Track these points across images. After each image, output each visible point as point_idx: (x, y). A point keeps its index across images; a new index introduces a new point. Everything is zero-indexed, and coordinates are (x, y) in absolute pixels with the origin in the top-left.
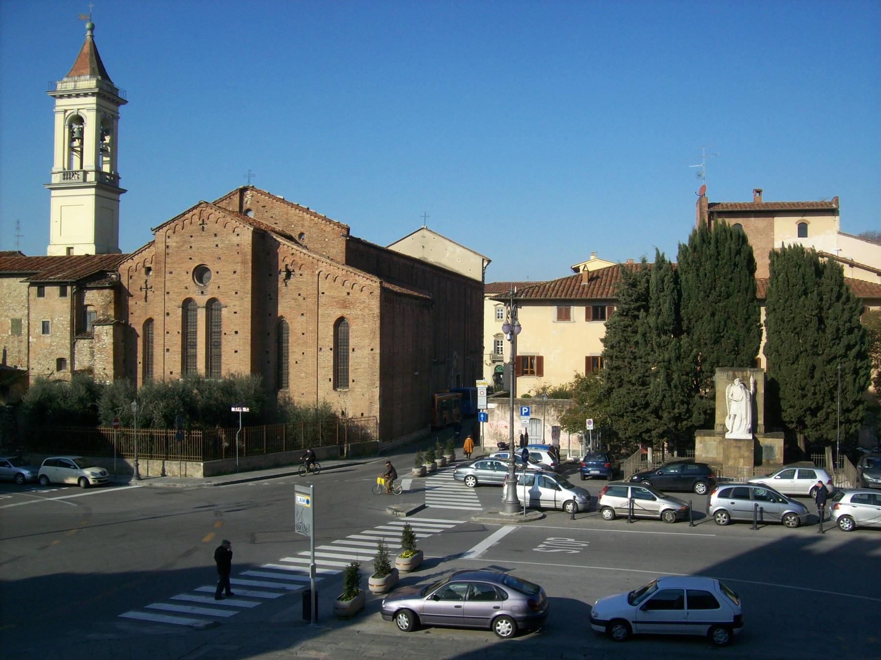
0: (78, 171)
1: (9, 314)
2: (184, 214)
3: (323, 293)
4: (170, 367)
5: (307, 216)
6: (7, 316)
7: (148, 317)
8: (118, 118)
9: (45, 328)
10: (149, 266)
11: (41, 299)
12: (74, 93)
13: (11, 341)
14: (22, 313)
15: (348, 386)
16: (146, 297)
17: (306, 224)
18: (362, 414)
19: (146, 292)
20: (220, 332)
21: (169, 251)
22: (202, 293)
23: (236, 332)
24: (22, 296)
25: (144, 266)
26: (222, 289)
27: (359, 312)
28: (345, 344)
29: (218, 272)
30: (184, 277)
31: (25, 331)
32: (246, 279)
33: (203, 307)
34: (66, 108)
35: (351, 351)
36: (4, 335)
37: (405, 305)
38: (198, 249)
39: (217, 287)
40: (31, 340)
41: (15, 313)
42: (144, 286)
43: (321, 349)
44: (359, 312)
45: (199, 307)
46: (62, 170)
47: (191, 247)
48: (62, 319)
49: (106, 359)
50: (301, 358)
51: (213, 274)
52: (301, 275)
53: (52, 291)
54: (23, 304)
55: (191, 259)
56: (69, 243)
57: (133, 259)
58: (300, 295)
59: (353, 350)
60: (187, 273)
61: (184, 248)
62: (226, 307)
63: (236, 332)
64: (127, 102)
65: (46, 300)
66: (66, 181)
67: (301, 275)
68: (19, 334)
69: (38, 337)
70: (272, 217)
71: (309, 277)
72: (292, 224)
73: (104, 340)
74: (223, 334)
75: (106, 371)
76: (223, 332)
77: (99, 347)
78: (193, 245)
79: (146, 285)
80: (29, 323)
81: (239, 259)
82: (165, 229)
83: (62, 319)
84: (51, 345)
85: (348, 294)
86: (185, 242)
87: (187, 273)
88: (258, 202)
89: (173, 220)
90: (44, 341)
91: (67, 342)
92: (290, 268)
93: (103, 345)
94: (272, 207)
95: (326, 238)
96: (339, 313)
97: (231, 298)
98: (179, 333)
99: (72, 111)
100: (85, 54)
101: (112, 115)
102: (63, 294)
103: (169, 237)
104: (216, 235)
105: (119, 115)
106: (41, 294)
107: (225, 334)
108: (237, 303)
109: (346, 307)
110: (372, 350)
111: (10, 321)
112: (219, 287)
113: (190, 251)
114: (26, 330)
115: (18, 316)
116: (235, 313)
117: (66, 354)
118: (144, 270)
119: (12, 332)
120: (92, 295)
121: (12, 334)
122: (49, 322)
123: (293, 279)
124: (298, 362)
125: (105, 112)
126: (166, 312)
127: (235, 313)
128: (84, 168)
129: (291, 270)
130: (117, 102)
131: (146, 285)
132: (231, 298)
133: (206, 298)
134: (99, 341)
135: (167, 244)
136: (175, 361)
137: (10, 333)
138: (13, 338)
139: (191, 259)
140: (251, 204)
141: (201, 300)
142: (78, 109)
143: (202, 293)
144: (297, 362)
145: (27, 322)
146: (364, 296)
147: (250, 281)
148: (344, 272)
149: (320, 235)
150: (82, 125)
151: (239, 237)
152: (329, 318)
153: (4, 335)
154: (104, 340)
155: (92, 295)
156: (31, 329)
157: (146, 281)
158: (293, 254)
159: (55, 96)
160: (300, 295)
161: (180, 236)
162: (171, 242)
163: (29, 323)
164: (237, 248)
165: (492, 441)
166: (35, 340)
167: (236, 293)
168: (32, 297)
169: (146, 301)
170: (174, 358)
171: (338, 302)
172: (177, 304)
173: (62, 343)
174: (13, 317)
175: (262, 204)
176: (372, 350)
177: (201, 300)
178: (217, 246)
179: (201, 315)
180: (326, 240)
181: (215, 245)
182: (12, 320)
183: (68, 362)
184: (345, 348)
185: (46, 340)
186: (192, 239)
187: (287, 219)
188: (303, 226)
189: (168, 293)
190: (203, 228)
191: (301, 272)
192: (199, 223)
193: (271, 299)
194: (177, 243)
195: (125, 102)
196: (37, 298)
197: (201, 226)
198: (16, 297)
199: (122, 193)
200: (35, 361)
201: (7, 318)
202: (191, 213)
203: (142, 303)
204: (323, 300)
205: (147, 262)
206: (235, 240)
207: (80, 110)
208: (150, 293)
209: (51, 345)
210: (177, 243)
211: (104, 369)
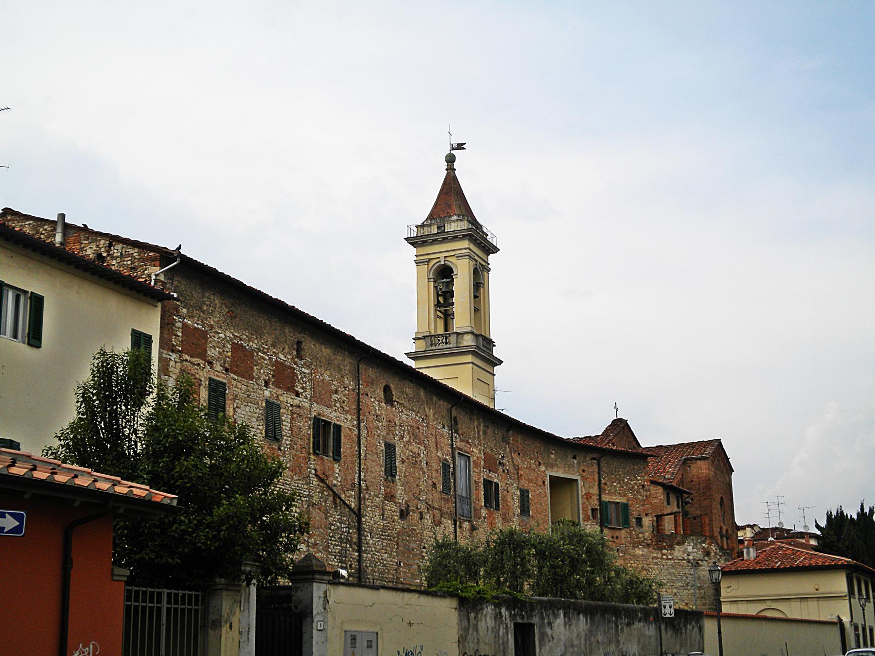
8: (489, 270)
66: (433, 348)
99: (438, 260)
101: (482, 265)
105: (489, 266)
142: (445, 257)
207: (447, 259)
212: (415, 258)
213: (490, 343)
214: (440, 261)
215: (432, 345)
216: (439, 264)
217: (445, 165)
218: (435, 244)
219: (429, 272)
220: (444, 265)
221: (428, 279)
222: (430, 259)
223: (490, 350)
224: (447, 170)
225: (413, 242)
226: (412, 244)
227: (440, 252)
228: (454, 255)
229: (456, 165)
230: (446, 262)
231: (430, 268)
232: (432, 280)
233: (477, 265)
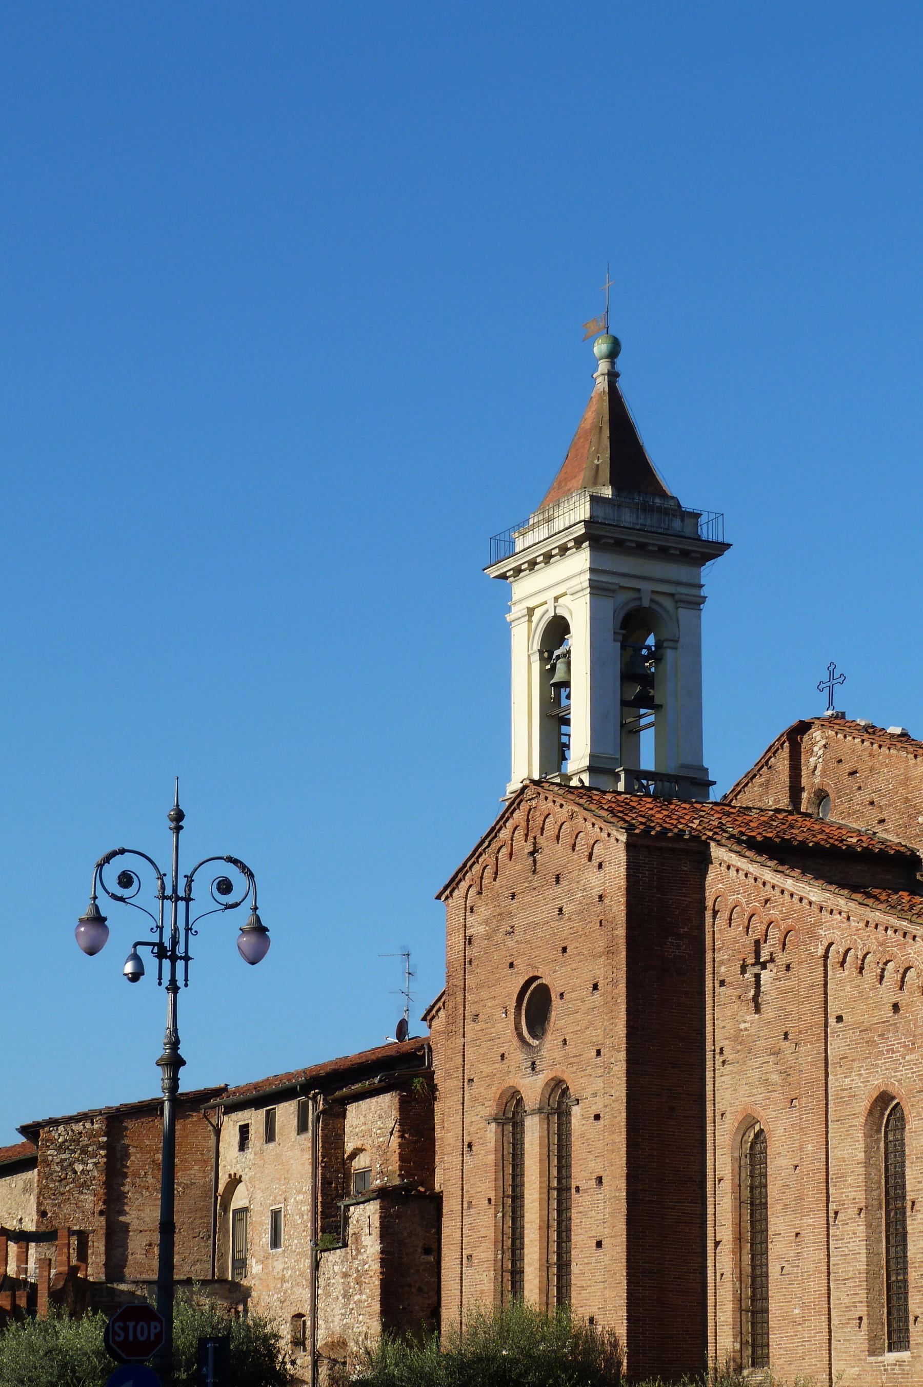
2: (494, 832)
11: (271, 1145)
21: (474, 951)
23: (600, 1180)
34: (531, 603)
64: (729, 545)
69: (263, 1261)
74: (573, 1191)
76: (574, 1185)
78: (516, 922)
81: (601, 945)
88: (840, 761)
89: (476, 854)
91: (306, 1263)
98: (490, 1200)
126: (467, 1139)
142: (556, 599)
147: (623, 1007)
159: (503, 576)
164: (598, 908)
167: (598, 1053)
187: (907, 800)
189: (470, 1080)
192: (526, 851)
194: (487, 922)
195: (719, 548)
209: (283, 1280)
210: (487, 922)
230: (560, 612)
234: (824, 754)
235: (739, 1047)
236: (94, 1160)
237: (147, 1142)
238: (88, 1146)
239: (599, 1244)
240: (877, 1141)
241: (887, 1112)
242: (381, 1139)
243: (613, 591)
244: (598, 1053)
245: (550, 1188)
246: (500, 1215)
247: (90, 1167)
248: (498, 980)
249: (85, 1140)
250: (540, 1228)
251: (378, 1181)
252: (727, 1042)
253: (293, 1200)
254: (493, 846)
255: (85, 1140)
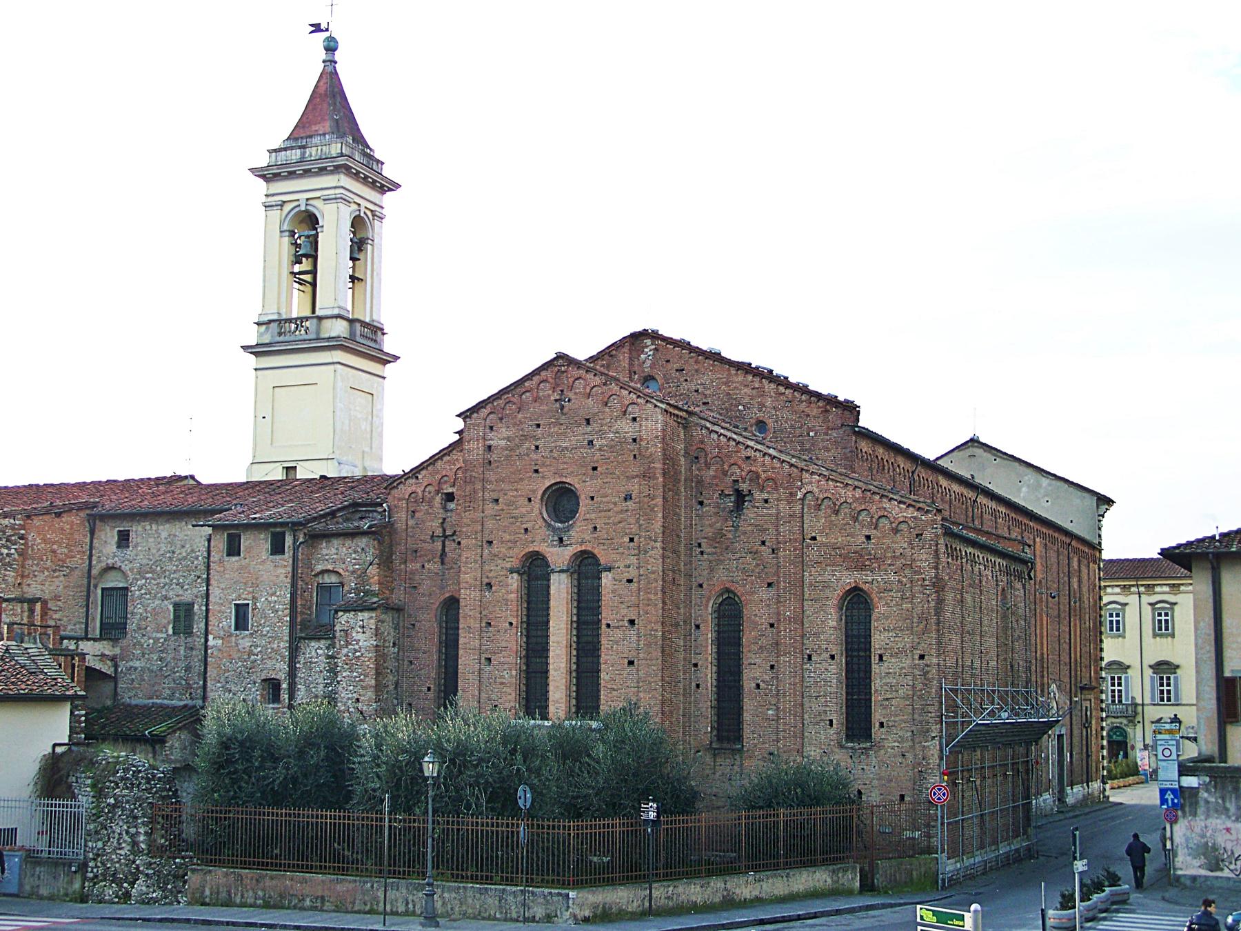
0: (307, 319)
1: (171, 594)
3: (814, 538)
4: (494, 697)
5: (770, 387)
6: (165, 598)
7: (447, 595)
9: (241, 619)
10: (450, 490)
11: (234, 559)
12: (299, 169)
13: (173, 647)
14: (195, 591)
15: (869, 737)
16: (443, 553)
17: (769, 402)
18: (902, 797)
19: (444, 543)
20: (600, 621)
22: (561, 540)
24: (197, 558)
25: (438, 492)
26: (602, 534)
27: (892, 577)
28: (862, 646)
29: (592, 498)
30: (524, 510)
31: (198, 627)
32: (652, 510)
33: (562, 571)
34: (285, 198)
35: (875, 659)
36: (159, 635)
37: (982, 567)
38: (551, 451)
39: (591, 527)
40: (211, 643)
41: (181, 592)
42: (439, 532)
43: (810, 657)
44: (892, 577)
45: (553, 571)
46: (275, 317)
47: (537, 447)
48: (274, 598)
49: (361, 680)
50: (767, 678)
51: (584, 502)
52: (766, 501)
53: (256, 546)
54: (198, 573)
55: (536, 471)
56: (290, 456)
57: (417, 478)
58: (763, 543)
59: (881, 657)
60: (530, 500)
61: (523, 450)
62: (609, 569)
63: (632, 622)
65: (243, 563)
66: (282, 338)
67: (766, 501)
68: (188, 632)
70: (697, 391)
71: (783, 504)
72: (740, 404)
73: (358, 641)
74: (604, 627)
75: (360, 705)
76: (604, 622)
77: (347, 655)
78: (540, 443)
79: (444, 530)
80: (207, 611)
82: (484, 412)
83: (274, 598)
84: (251, 653)
85: (868, 538)
86: (525, 437)
87: (530, 500)
90: (237, 645)
92: (744, 487)
93: (356, 651)
94: (697, 371)
95: (810, 430)
96: (848, 580)
97: (621, 550)
98: (511, 624)
99: (296, 204)
100: (321, 94)
101: (372, 211)
102: (278, 549)
103: (491, 428)
104: (588, 421)
105: (384, 211)
106: (233, 549)
107: (608, 626)
108: (633, 560)
109: (862, 568)
110: (922, 657)
111: (171, 608)
112: (595, 528)
113: (533, 456)
114: (202, 625)
115: (187, 597)
116: (630, 581)
117: (280, 670)
118: (438, 499)
119: (174, 628)
120: (334, 551)
121: (174, 633)
122: (248, 604)
123: (749, 512)
124: (762, 685)
125: (359, 205)
127: (630, 581)
128: (319, 313)
129: (746, 492)
130: (383, 186)
131: (444, 530)
132: (621, 550)
133: (569, 551)
134: (348, 644)
135: (488, 443)
136: (502, 683)
137: (170, 632)
138: (176, 641)
139: (536, 471)
140: (653, 366)
141: (559, 556)
142: (307, 199)
143: (561, 540)
144: (758, 686)
145: (204, 608)
146: (901, 544)
148: (858, 493)
149: (798, 425)
150: (316, 229)
151: (637, 424)
152: (827, 591)
153: (159, 635)
154: (358, 641)
155: (334, 551)
156: (213, 620)
157: (444, 519)
158: (748, 458)
160: (763, 543)
161: (515, 424)
162: (498, 440)
163: (207, 611)
164: (633, 446)
165: (1196, 863)
166: (220, 642)
168: (215, 556)
169: (443, 563)
170: (501, 677)
171: (845, 558)
172: (509, 565)
173: (272, 649)
174: (177, 599)
175: (677, 366)
176: (922, 657)
177: (559, 556)
178: (591, 442)
179: (560, 589)
180: (812, 434)
181: (586, 443)
182: (176, 605)
183: (284, 686)
184: (862, 654)
185: (240, 641)
186: (539, 431)
187: (729, 394)
188: (762, 406)
189: (490, 543)
190: (562, 407)
191: (765, 496)
192: (552, 398)
193: (702, 553)
194: (508, 439)
196: (227, 559)
197: (558, 405)
198: (185, 558)
199: (390, 362)
200: (219, 685)
201: (166, 602)
202: (536, 379)
203: (434, 566)
204: (813, 554)
205: (446, 482)
206: (629, 429)
207: (311, 202)
208: (450, 546)
209: (251, 653)
210: (508, 439)
211: (358, 700)
212: (264, 199)
213: (376, 330)
214: (299, 206)
215: (280, 334)
216: (297, 209)
217: (323, 55)
218: (293, 178)
219: (281, 224)
220: (307, 211)
221: (281, 232)
222: (284, 202)
223: (375, 341)
224: (324, 62)
225: (267, 175)
226: (263, 177)
227: (299, 190)
228: (319, 198)
229: (338, 56)
230: (309, 208)
231: (283, 217)
232: (287, 234)
233: (360, 210)
234: (654, 354)
235: (717, 545)
236: (15, 547)
237: (48, 536)
238: (11, 536)
239: (631, 663)
240: (841, 615)
241: (848, 599)
242: (357, 567)
243: (350, 202)
244: (632, 540)
245: (572, 622)
246: (519, 634)
247: (13, 551)
248: (522, 479)
249: (9, 532)
250: (567, 647)
251: (353, 595)
252: (705, 540)
253: (263, 599)
254: (518, 390)
255: (9, 532)
